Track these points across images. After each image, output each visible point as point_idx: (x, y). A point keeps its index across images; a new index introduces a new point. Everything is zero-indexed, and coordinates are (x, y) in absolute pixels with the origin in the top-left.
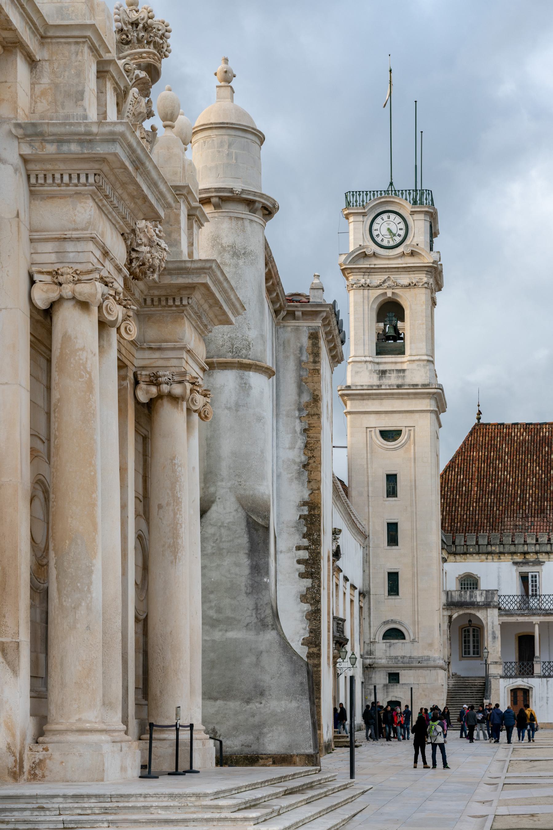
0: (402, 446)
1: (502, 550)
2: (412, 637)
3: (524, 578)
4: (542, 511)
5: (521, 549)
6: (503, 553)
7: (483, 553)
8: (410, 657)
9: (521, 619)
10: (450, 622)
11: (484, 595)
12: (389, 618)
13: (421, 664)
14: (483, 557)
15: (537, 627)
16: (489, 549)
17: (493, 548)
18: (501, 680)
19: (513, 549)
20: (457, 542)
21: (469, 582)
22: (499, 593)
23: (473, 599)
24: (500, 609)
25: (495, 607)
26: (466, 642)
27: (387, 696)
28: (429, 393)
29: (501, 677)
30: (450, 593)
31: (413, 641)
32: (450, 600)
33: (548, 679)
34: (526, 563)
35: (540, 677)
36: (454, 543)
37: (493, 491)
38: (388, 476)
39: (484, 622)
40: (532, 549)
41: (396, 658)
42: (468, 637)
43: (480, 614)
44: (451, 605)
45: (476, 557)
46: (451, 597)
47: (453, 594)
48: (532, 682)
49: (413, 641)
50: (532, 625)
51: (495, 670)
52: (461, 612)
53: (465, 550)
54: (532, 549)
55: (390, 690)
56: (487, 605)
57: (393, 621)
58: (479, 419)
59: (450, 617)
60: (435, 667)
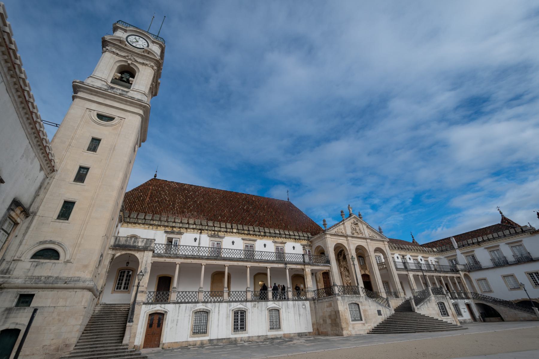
0: (112, 125)
1: (159, 224)
2: (68, 258)
3: (170, 241)
4: (183, 212)
5: (171, 224)
6: (160, 226)
7: (147, 224)
8: (57, 278)
9: (168, 260)
10: (112, 259)
11: (145, 242)
12: (48, 239)
13: (67, 285)
14: (147, 226)
16: (152, 222)
17: (154, 222)
18: (144, 306)
19: (166, 224)
20: (132, 216)
22: (155, 242)
23: (136, 244)
24: (154, 252)
25: (151, 250)
26: (121, 280)
27: (5, 322)
28: (141, 105)
29: (144, 304)
30: (118, 238)
31: (68, 262)
32: (117, 243)
33: (181, 305)
34: (173, 232)
35: (174, 303)
36: (129, 217)
37: (158, 201)
38: (94, 139)
39: (140, 261)
40: (178, 225)
41: (39, 278)
42: (124, 273)
43: (138, 255)
44: (117, 247)
45: (143, 226)
46: (119, 241)
47: (121, 239)
48: (169, 308)
49: (68, 262)
51: (141, 298)
52: (124, 252)
53: (136, 222)
54: (178, 225)
55: (12, 315)
56: (145, 249)
57: (51, 242)
58: (155, 176)
59: (114, 255)
60: (83, 288)
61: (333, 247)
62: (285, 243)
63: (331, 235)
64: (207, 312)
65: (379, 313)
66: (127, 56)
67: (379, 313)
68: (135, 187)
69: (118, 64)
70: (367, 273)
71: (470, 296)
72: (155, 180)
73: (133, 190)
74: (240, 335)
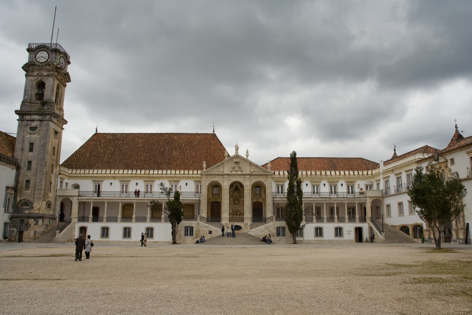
4: (109, 162)
15: (92, 204)
18: (76, 224)
21: (77, 187)
37: (94, 156)
50: (90, 203)
58: (97, 131)
61: (207, 185)
62: (178, 181)
63: (206, 175)
64: (107, 229)
65: (210, 232)
66: (38, 74)
68: (81, 145)
69: (34, 83)
70: (260, 200)
71: (368, 221)
72: (96, 134)
73: (80, 148)
74: (127, 240)
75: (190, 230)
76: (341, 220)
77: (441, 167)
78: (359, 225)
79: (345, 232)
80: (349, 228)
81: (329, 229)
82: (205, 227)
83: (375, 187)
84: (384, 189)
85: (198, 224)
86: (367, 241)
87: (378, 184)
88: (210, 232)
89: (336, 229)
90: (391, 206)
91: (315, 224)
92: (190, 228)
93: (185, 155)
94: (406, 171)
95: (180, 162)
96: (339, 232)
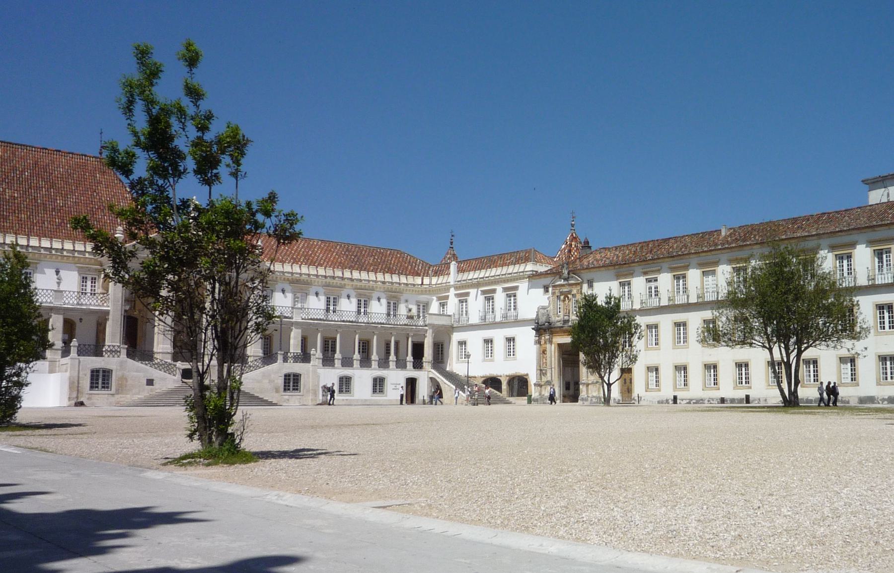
67: (150, 382)
71: (427, 366)
75: (104, 376)
76: (384, 363)
77: (570, 292)
78: (412, 373)
79: (388, 386)
80: (396, 378)
81: (362, 378)
82: (137, 371)
83: (434, 308)
84: (457, 313)
85: (122, 364)
86: (424, 403)
87: (443, 305)
88: (150, 382)
89: (375, 380)
90: (468, 344)
91: (338, 371)
92: (104, 371)
93: (36, 201)
94: (505, 289)
95: (29, 218)
96: (378, 384)
